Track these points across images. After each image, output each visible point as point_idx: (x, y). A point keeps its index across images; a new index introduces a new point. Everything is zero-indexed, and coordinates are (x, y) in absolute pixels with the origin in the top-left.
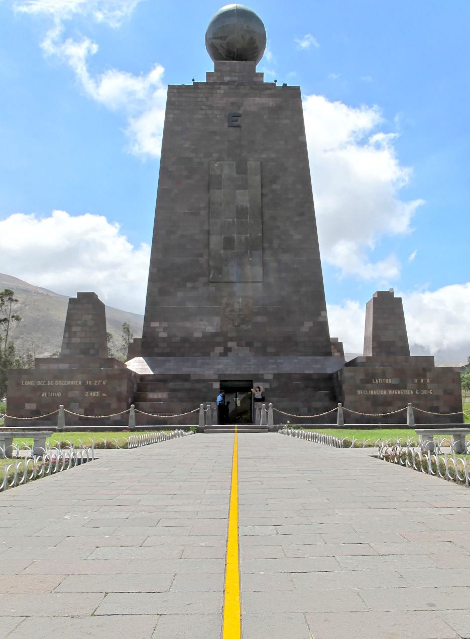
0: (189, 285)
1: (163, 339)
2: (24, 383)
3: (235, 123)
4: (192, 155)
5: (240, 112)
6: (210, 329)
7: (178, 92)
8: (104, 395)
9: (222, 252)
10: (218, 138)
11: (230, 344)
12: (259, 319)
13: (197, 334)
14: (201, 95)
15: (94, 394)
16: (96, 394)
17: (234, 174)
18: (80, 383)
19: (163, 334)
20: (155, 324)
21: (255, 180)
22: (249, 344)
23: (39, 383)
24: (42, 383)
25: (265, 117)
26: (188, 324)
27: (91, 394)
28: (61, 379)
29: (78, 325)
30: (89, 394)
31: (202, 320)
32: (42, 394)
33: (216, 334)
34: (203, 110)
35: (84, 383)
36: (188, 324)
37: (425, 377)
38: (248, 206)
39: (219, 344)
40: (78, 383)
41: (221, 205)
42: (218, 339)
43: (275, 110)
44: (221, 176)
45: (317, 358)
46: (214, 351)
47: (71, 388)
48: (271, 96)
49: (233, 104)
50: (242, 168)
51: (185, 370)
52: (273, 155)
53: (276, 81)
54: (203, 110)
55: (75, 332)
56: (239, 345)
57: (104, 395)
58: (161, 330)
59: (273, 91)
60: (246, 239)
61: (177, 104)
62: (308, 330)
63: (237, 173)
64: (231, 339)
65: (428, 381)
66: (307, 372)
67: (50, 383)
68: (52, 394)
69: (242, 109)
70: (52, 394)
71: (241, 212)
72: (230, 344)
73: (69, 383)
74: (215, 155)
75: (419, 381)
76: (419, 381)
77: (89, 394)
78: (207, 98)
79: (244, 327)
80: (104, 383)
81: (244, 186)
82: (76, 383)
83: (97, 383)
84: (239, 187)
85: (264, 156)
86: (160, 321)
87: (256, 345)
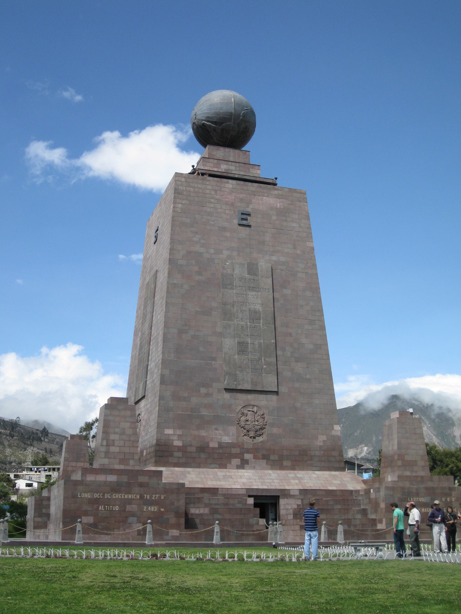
0: (203, 390)
1: (179, 449)
2: (80, 495)
3: (244, 222)
4: (202, 250)
5: (249, 210)
6: (226, 439)
7: (186, 182)
8: (162, 510)
9: (236, 357)
10: (228, 234)
11: (247, 456)
12: (275, 430)
13: (213, 445)
14: (209, 187)
15: (153, 509)
16: (154, 509)
18: (138, 497)
19: (178, 443)
20: (169, 431)
22: (266, 457)
23: (96, 496)
24: (99, 495)
25: (274, 218)
26: (203, 433)
27: (149, 509)
28: (118, 491)
29: (115, 433)
30: (147, 509)
31: (216, 429)
32: (98, 507)
34: (212, 203)
35: (142, 497)
36: (203, 433)
37: (450, 495)
38: (261, 310)
40: (136, 496)
41: (233, 306)
42: (235, 451)
43: (283, 213)
44: (233, 275)
45: (333, 473)
46: (230, 463)
47: (130, 502)
48: (278, 197)
49: (241, 200)
50: (252, 269)
51: (210, 484)
52: (283, 259)
53: (276, 179)
54: (212, 203)
56: (255, 457)
57: (162, 510)
58: (176, 438)
59: (280, 192)
60: (260, 344)
61: (185, 193)
62: (322, 444)
63: (249, 273)
64: (248, 451)
65: (453, 499)
66: (330, 488)
67: (107, 496)
68: (110, 507)
69: (251, 206)
70: (110, 507)
71: (255, 316)
72: (247, 456)
73: (126, 497)
74: (226, 253)
75: (446, 500)
76: (446, 500)
77: (147, 509)
78: (216, 191)
80: (162, 498)
82: (133, 496)
83: (155, 497)
84: (253, 289)
85: (274, 258)
86: (174, 428)
87: (272, 457)
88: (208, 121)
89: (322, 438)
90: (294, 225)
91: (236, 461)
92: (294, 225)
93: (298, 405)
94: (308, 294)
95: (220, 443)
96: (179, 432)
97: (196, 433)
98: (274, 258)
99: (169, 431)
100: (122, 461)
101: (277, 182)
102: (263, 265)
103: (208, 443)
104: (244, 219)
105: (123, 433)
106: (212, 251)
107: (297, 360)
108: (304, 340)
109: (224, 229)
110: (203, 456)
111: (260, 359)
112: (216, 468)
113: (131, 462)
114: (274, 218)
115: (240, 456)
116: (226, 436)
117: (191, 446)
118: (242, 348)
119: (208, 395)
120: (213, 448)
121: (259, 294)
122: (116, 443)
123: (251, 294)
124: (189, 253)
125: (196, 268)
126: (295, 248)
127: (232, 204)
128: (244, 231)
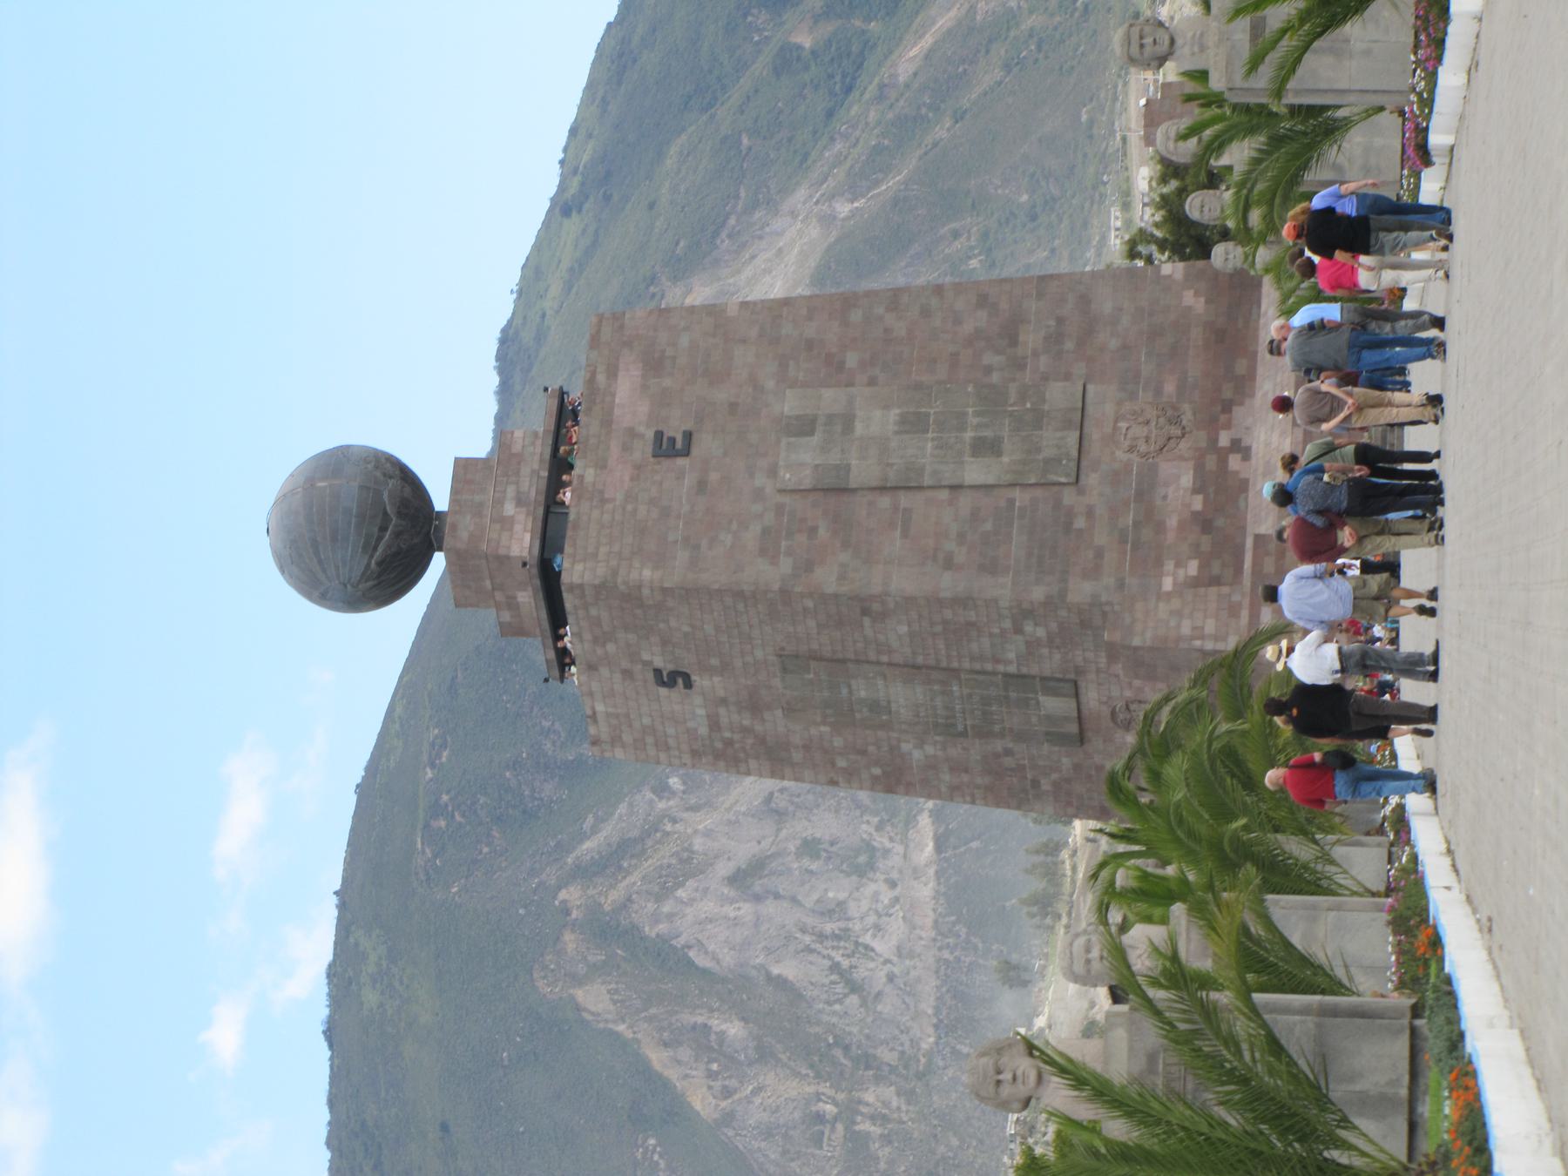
0: (1080, 523)
4: (755, 529)
5: (650, 434)
6: (1187, 480)
7: (584, 560)
9: (1005, 459)
10: (714, 476)
11: (1224, 440)
12: (1170, 388)
13: (1198, 503)
17: (816, 439)
21: (831, 399)
22: (1227, 407)
25: (667, 382)
26: (1172, 522)
29: (1179, 626)
31: (1165, 497)
33: (1199, 469)
36: (1172, 522)
38: (897, 411)
39: (1223, 462)
42: (1211, 462)
43: (654, 364)
46: (1237, 473)
48: (612, 373)
49: (626, 448)
50: (804, 426)
55: (1194, 628)
56: (1228, 426)
58: (1181, 572)
59: (601, 368)
60: (977, 414)
61: (614, 563)
62: (1202, 300)
63: (811, 433)
64: (1214, 441)
69: (642, 429)
71: (913, 424)
72: (1224, 440)
74: (760, 480)
78: (603, 501)
79: (1188, 418)
81: (848, 421)
85: (770, 384)
86: (1161, 575)
87: (1227, 393)
88: (375, 549)
89: (1189, 298)
90: (684, 341)
91: (1234, 462)
92: (684, 341)
93: (1114, 344)
94: (856, 316)
95: (1196, 491)
96: (1169, 566)
97: (1171, 537)
98: (770, 384)
99: (1168, 584)
100: (1234, 611)
101: (554, 386)
102: (791, 404)
103: (1195, 514)
104: (667, 448)
105: (1179, 614)
106: (757, 508)
107: (1014, 342)
108: (968, 327)
109: (701, 486)
110: (1220, 522)
111: (1011, 414)
112: (1246, 499)
113: (1236, 598)
114: (667, 382)
115: (1222, 457)
116: (1179, 486)
117: (1198, 545)
118: (986, 447)
119: (1090, 513)
120: (1205, 502)
121: (859, 413)
122: (1199, 624)
123: (859, 428)
124: (763, 552)
125: (802, 538)
126: (744, 341)
127: (638, 467)
128: (706, 445)
